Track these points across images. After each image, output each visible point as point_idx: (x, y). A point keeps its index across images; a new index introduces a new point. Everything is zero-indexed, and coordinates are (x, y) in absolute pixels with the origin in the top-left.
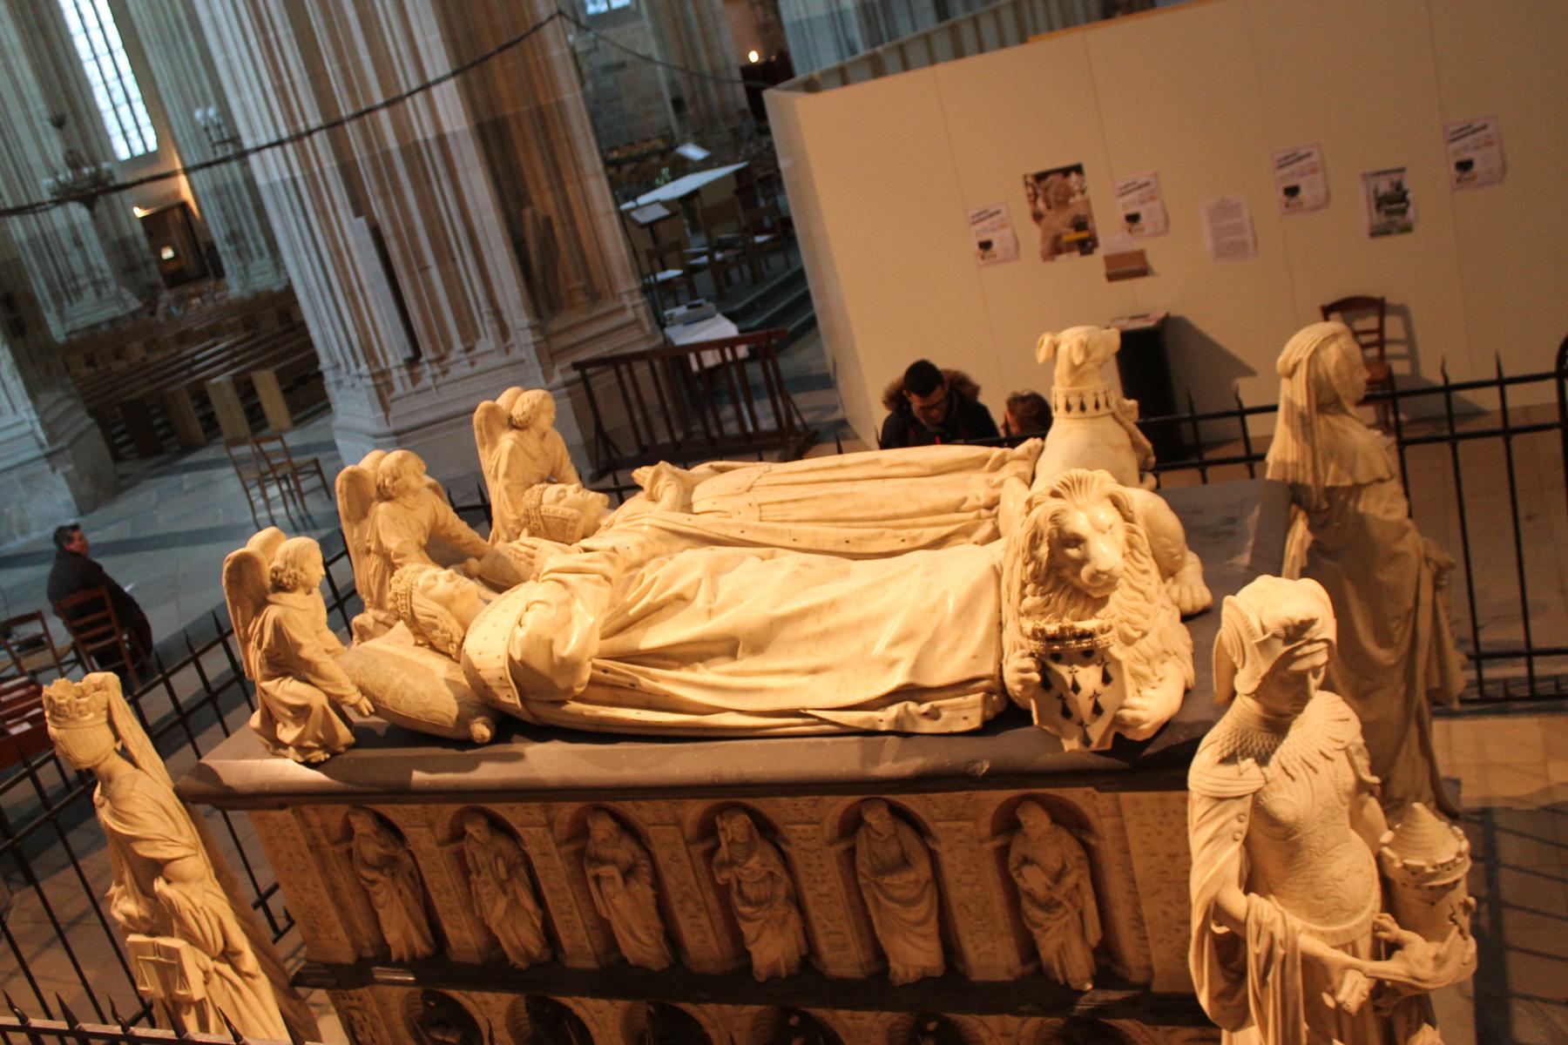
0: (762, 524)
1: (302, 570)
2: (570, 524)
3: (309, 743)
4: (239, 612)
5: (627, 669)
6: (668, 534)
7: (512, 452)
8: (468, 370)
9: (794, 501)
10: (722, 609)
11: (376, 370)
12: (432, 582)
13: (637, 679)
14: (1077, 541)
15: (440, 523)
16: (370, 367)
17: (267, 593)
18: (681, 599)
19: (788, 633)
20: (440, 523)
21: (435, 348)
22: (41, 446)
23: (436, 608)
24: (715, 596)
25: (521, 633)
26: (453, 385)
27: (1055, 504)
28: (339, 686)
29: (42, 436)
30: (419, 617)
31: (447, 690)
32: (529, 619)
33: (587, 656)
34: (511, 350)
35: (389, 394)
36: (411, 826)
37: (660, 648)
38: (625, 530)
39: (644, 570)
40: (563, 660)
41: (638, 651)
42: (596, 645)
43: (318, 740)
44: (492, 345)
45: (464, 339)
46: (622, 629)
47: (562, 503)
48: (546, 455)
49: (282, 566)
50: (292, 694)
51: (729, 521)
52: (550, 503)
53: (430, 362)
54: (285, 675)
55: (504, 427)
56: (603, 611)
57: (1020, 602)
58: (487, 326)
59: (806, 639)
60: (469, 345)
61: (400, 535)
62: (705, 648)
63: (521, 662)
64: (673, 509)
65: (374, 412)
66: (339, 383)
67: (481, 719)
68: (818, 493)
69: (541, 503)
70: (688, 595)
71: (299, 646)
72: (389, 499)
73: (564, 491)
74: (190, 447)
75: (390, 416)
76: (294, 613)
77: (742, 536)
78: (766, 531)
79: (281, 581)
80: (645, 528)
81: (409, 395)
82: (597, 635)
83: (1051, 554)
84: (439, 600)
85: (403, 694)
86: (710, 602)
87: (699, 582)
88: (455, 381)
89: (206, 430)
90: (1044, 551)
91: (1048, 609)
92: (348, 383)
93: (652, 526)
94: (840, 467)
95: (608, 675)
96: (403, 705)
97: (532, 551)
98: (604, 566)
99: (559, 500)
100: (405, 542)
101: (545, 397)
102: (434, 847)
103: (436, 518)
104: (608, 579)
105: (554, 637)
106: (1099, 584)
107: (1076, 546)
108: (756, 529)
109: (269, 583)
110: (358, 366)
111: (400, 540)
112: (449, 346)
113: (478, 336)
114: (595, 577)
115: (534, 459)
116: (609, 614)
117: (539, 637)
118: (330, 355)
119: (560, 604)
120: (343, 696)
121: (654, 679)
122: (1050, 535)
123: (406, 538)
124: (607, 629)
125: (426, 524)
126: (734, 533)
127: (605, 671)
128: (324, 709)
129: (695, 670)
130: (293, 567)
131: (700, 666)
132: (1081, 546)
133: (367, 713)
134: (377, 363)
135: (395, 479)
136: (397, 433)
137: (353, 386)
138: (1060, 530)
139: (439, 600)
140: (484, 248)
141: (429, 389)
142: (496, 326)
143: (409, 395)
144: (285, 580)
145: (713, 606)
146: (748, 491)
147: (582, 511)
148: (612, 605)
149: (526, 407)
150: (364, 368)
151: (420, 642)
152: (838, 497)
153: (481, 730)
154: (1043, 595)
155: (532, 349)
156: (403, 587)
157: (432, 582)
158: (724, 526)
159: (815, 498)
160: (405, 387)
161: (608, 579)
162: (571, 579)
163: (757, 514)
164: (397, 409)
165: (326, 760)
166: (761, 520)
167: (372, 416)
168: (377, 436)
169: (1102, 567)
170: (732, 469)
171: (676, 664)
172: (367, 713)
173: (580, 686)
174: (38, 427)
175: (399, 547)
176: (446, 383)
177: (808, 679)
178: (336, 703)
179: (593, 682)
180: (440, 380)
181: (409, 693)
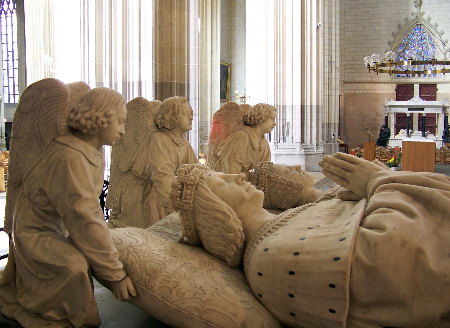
1: (106, 115)
3: (52, 314)
17: (58, 134)
28: (108, 255)
43: (63, 311)
79: (78, 121)
85: (178, 284)
109: (63, 124)
115: (254, 149)
120: (107, 268)
128: (83, 274)
144: (83, 121)
172: (126, 296)
181: (184, 284)
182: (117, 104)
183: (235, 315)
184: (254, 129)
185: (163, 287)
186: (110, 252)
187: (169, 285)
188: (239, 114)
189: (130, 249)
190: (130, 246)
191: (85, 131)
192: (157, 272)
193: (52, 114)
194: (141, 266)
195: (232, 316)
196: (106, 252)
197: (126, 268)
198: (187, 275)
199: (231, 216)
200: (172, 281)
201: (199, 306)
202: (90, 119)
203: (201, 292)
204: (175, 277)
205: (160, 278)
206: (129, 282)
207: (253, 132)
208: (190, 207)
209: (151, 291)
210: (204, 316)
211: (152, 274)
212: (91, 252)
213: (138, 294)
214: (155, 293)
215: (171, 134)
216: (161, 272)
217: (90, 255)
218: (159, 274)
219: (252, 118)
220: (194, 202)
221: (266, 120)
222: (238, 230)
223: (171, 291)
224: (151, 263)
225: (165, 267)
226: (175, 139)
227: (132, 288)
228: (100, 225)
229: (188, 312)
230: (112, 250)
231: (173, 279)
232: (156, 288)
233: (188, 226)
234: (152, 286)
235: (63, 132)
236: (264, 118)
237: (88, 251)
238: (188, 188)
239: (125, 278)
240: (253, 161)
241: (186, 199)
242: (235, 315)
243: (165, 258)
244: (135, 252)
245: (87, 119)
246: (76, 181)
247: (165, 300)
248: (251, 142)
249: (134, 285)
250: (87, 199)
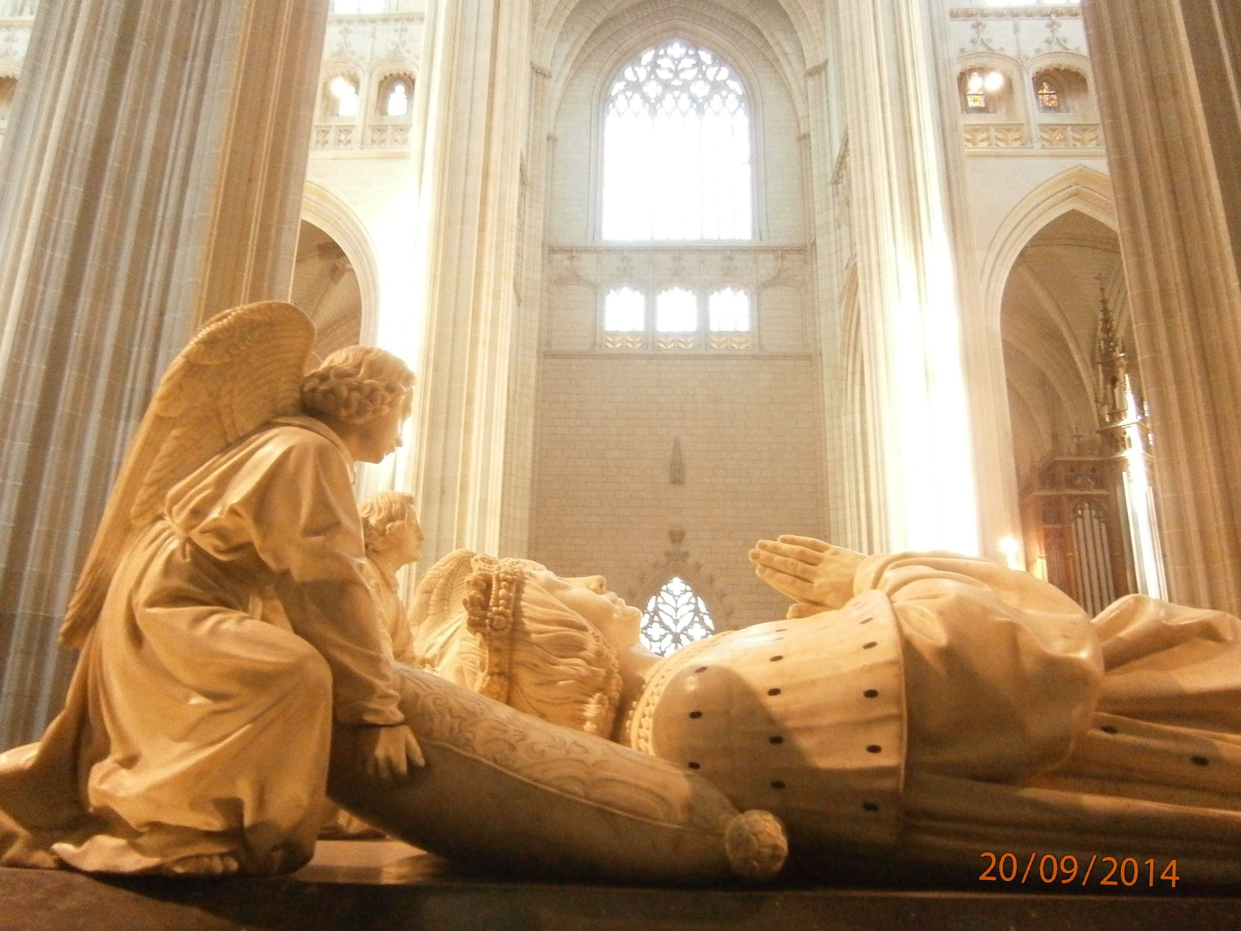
4: (165, 448)
144: (345, 391)
165: (226, 877)
185: (492, 740)
187: (506, 737)
192: (474, 714)
193: (271, 372)
194: (438, 701)
208: (507, 623)
209: (466, 750)
211: (463, 716)
213: (428, 764)
214: (474, 752)
220: (514, 615)
223: (513, 747)
229: (557, 787)
233: (497, 665)
234: (467, 740)
241: (498, 606)
245: (351, 389)
247: (499, 764)
249: (420, 743)
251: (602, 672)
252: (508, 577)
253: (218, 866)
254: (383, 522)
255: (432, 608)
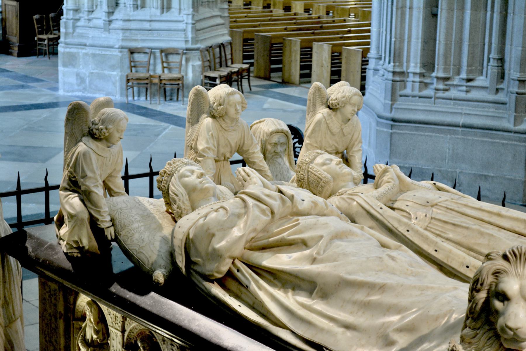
0: (426, 233)
1: (106, 129)
2: (322, 183)
5: (250, 275)
6: (364, 212)
7: (319, 122)
8: (463, 95)
9: (454, 225)
10: (322, 261)
11: (398, 70)
12: (189, 174)
13: (250, 283)
14: (504, 297)
15: (244, 149)
16: (394, 66)
18: (304, 244)
19: (347, 294)
20: (244, 149)
21: (446, 70)
22: (187, 42)
23: (181, 190)
24: (324, 251)
25: (201, 221)
26: (448, 101)
27: (501, 264)
28: (99, 212)
29: (190, 35)
30: (170, 192)
31: (157, 244)
32: (213, 215)
33: (228, 254)
34: (500, 91)
35: (400, 91)
36: (112, 327)
37: (273, 269)
38: (343, 199)
39: (301, 218)
40: (214, 250)
41: (261, 266)
42: (238, 251)
44: (486, 84)
45: (469, 72)
46: (263, 248)
47: (325, 167)
48: (344, 135)
49: (97, 122)
50: (71, 206)
51: (406, 220)
52: (317, 164)
53: (438, 78)
54: (74, 191)
55: (322, 104)
56: (255, 230)
57: (463, 329)
58: (492, 68)
59: (355, 303)
60: (471, 77)
61: (207, 142)
62: (297, 281)
63: (192, 240)
64: (379, 199)
65: (385, 98)
66: (376, 70)
67: (163, 270)
68: (471, 226)
69: (312, 162)
70: (309, 243)
71: (84, 177)
72: (213, 117)
73: (331, 160)
74: (285, 83)
75: (394, 106)
76: (94, 157)
77: (406, 234)
78: (422, 236)
79: (92, 130)
80: (355, 203)
81: (414, 96)
82: (242, 244)
83: (487, 302)
84: (185, 186)
85: (133, 235)
86: (318, 253)
87: (321, 237)
88: (451, 99)
89: (302, 76)
90: (482, 296)
91: (473, 341)
92: (381, 72)
93: (357, 202)
94: (499, 215)
95: (239, 275)
96: (129, 242)
97: (246, 177)
98: (276, 204)
99: (324, 164)
100: (209, 149)
101: (355, 94)
102: (120, 347)
103: (244, 143)
104: (272, 213)
105: (217, 233)
106: (506, 336)
107: (503, 301)
108: (417, 232)
110: (389, 63)
111: (206, 146)
112: (458, 73)
113: (481, 73)
114: (264, 207)
115: (333, 134)
116: (260, 235)
117: (208, 229)
118: (378, 48)
119: (233, 214)
120: (98, 220)
121: (260, 287)
122: (491, 285)
123: (211, 146)
124: (254, 244)
125: (233, 145)
126: (402, 230)
127: (238, 271)
129: (286, 292)
130: (102, 125)
131: (290, 294)
132: (506, 302)
133: (109, 238)
134: (401, 65)
135: (220, 105)
136: (394, 120)
137: (383, 75)
138: (497, 285)
139: (185, 186)
140: (510, 10)
141: (431, 98)
142: (496, 70)
143: (414, 96)
144: (94, 131)
145: (319, 257)
146: (432, 206)
147: (334, 178)
148: (265, 230)
149: (339, 96)
150: (392, 64)
151: (170, 211)
152: (482, 234)
153: (159, 276)
154: (474, 329)
155: (514, 96)
156: (170, 169)
157: (189, 174)
158: (399, 221)
159: (467, 228)
160: (413, 90)
161: (272, 213)
162: (250, 202)
163: (426, 224)
164: (401, 103)
166: (426, 229)
167: (382, 99)
168: (380, 117)
169: (511, 324)
170: (447, 191)
171: (279, 284)
173: (218, 272)
174: (190, 27)
175: (203, 150)
176: (444, 99)
177: (341, 330)
178: (93, 222)
179: (230, 274)
180: (440, 94)
181: (137, 236)
182: (114, 121)
183: (150, 257)
184: (334, 113)
186: (102, 210)
188: (322, 96)
189: (119, 210)
190: (121, 209)
191: (96, 136)
195: (148, 257)
196: (99, 210)
197: (112, 220)
198: (142, 231)
199: (182, 199)
200: (131, 233)
201: (137, 249)
202: (98, 129)
203: (142, 241)
204: (134, 231)
205: (126, 230)
206: (112, 229)
207: (332, 116)
210: (138, 255)
212: (91, 209)
215: (221, 120)
216: (128, 226)
217: (90, 210)
218: (127, 227)
219: (331, 102)
221: (342, 106)
222: (184, 209)
224: (125, 221)
225: (132, 224)
226: (223, 126)
227: (113, 234)
228: (97, 193)
230: (102, 209)
231: (133, 232)
232: (122, 236)
235: (86, 134)
236: (340, 104)
237: (89, 208)
238: (166, 176)
239: (109, 227)
240: (336, 145)
241: (164, 183)
242: (150, 257)
243: (135, 219)
244: (121, 212)
246: (85, 166)
248: (328, 127)
250: (90, 178)
251: (180, 211)
252: (169, 173)
253: (75, 255)
254: (216, 105)
255: (311, 108)
